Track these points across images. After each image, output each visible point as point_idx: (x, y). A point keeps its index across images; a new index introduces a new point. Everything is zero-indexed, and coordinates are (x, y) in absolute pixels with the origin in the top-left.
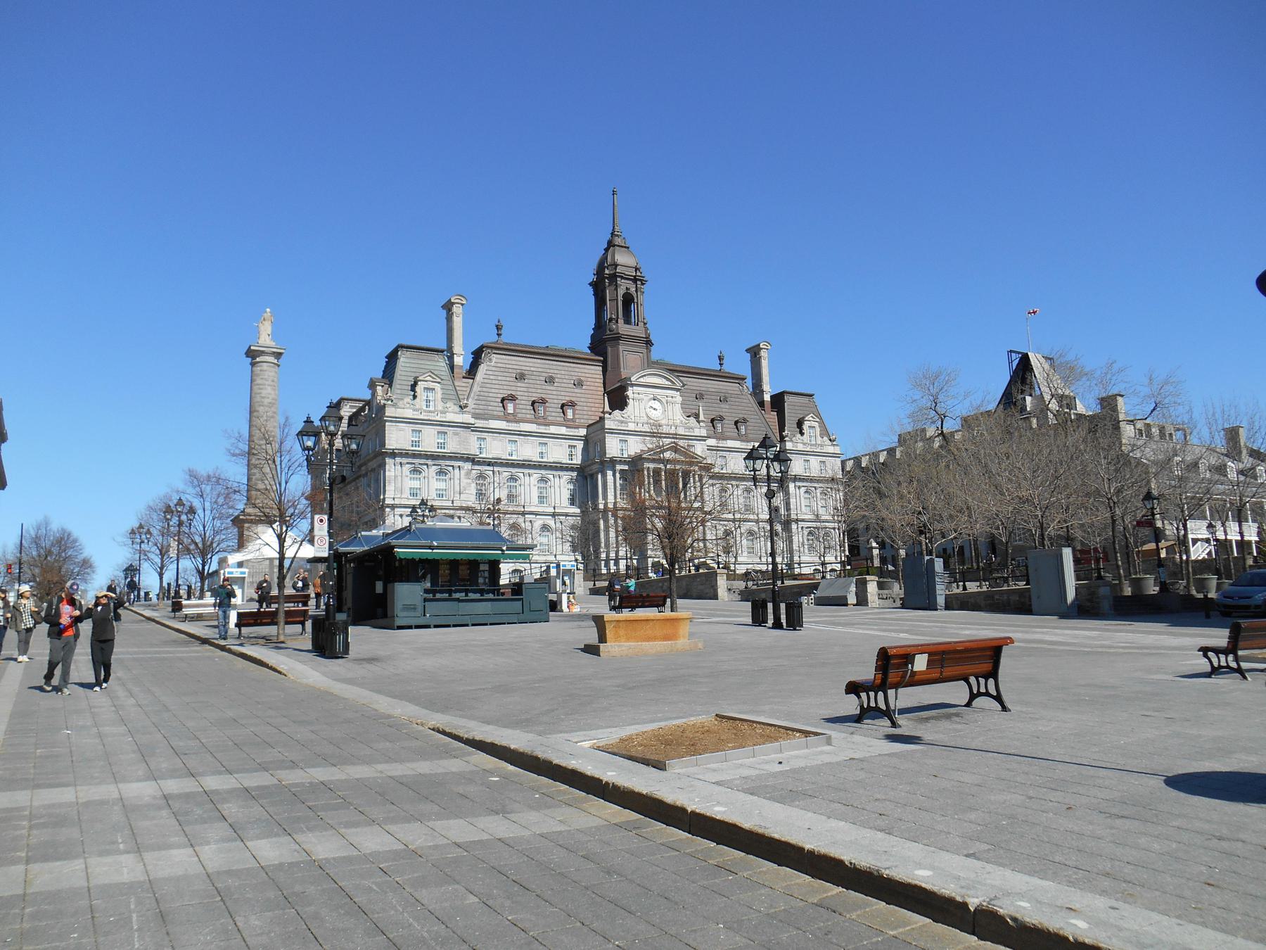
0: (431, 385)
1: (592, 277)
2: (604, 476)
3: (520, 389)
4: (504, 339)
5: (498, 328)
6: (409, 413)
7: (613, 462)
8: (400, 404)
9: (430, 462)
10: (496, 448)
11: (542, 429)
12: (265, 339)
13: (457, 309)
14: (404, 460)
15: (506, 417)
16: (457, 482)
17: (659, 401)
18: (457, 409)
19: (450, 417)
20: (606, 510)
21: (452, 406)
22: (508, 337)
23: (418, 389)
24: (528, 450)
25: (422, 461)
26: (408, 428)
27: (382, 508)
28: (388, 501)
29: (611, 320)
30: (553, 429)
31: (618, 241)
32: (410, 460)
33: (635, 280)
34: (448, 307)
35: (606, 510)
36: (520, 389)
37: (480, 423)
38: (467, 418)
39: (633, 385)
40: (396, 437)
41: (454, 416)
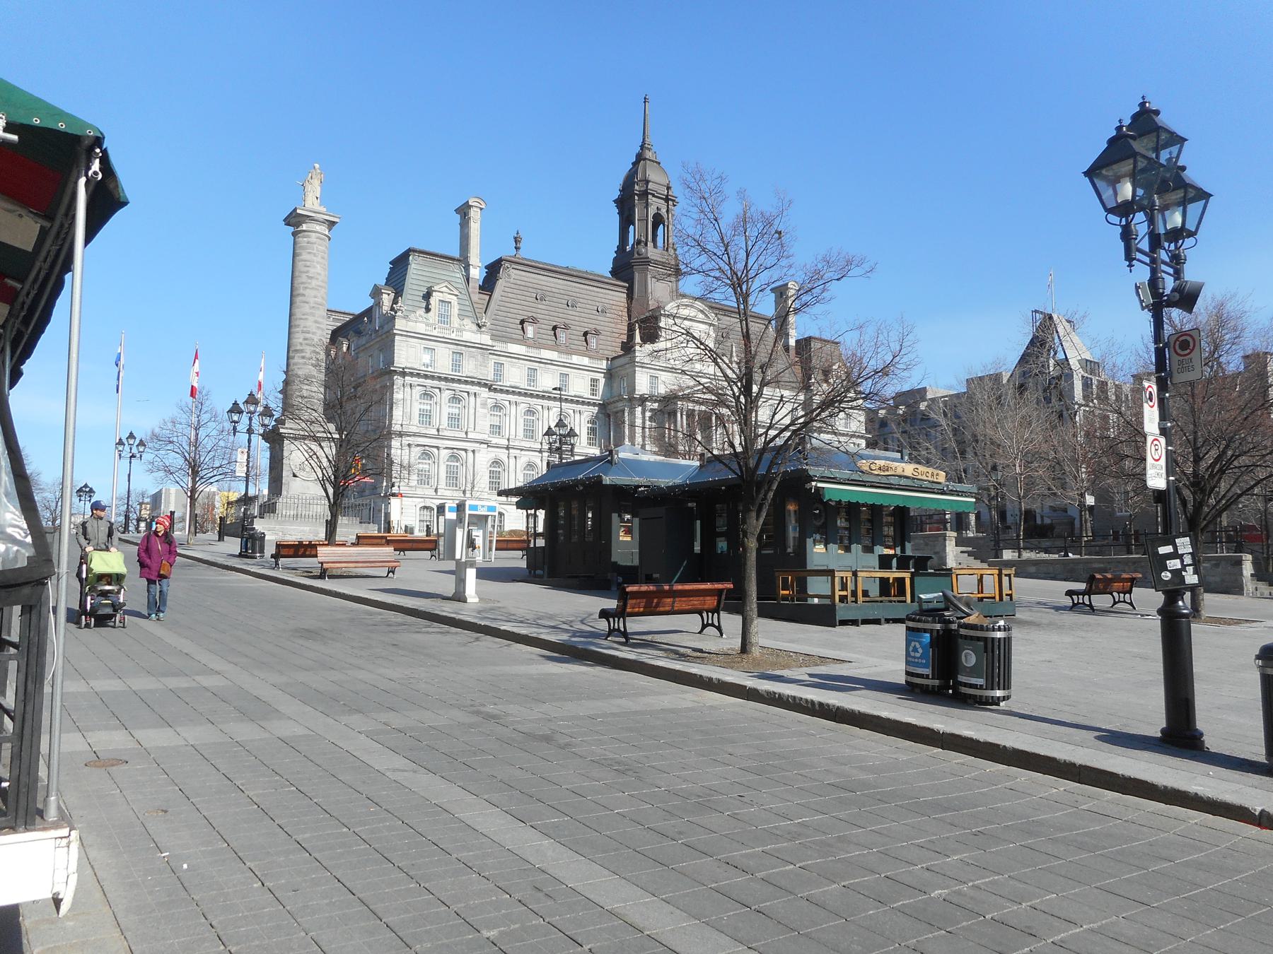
0: (448, 298)
1: (616, 194)
2: (632, 413)
3: (541, 310)
4: (523, 253)
5: (517, 240)
6: (421, 328)
7: (643, 400)
8: (412, 316)
9: (442, 384)
10: (515, 375)
11: (564, 358)
12: (312, 203)
13: (474, 214)
14: (415, 380)
15: (523, 341)
16: (472, 411)
18: (475, 328)
21: (469, 324)
22: (526, 253)
23: (432, 300)
25: (436, 383)
27: (389, 435)
28: (396, 428)
30: (575, 359)
31: (649, 155)
32: (422, 381)
33: (667, 200)
34: (464, 211)
36: (541, 310)
37: (499, 346)
38: (485, 339)
40: (406, 354)
41: (471, 335)
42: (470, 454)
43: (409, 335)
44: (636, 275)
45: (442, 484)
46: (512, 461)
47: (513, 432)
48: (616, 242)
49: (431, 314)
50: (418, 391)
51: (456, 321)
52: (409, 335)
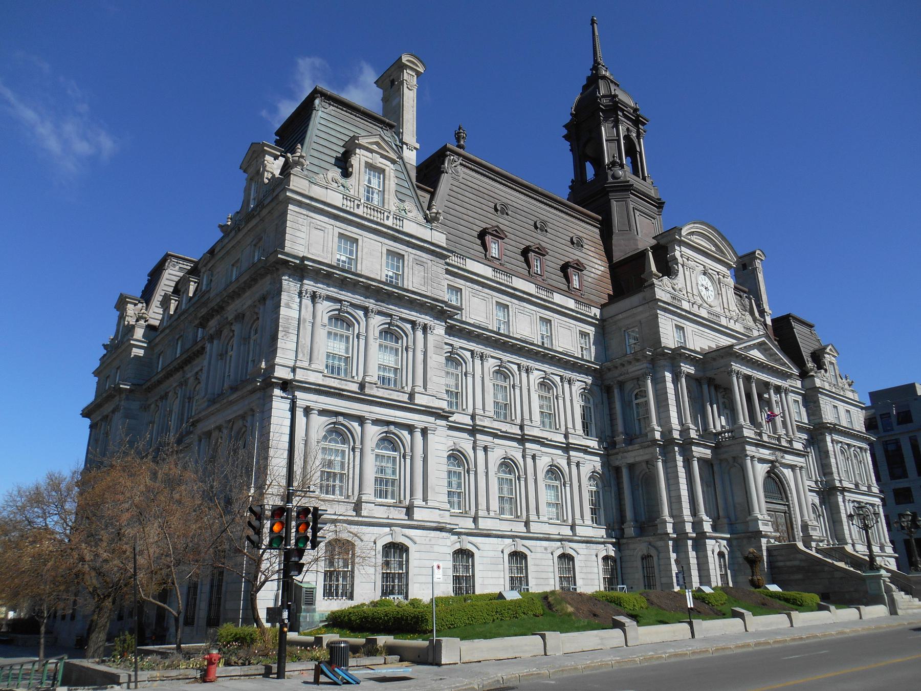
0: (379, 161)
2: (659, 383)
6: (336, 199)
7: (678, 356)
8: (320, 178)
9: (371, 303)
10: (478, 309)
11: (543, 294)
14: (322, 289)
16: (420, 357)
17: (711, 278)
18: (421, 218)
19: (410, 227)
20: (668, 442)
23: (354, 161)
24: (525, 325)
25: (358, 299)
26: (333, 228)
27: (268, 383)
28: (281, 373)
29: (613, 164)
32: (333, 292)
35: (668, 442)
38: (440, 238)
39: (681, 243)
40: (307, 237)
42: (418, 435)
43: (313, 206)
44: (614, 204)
45: (369, 493)
46: (481, 454)
47: (479, 404)
48: (571, 176)
49: (352, 181)
50: (325, 308)
51: (392, 204)
52: (313, 206)
